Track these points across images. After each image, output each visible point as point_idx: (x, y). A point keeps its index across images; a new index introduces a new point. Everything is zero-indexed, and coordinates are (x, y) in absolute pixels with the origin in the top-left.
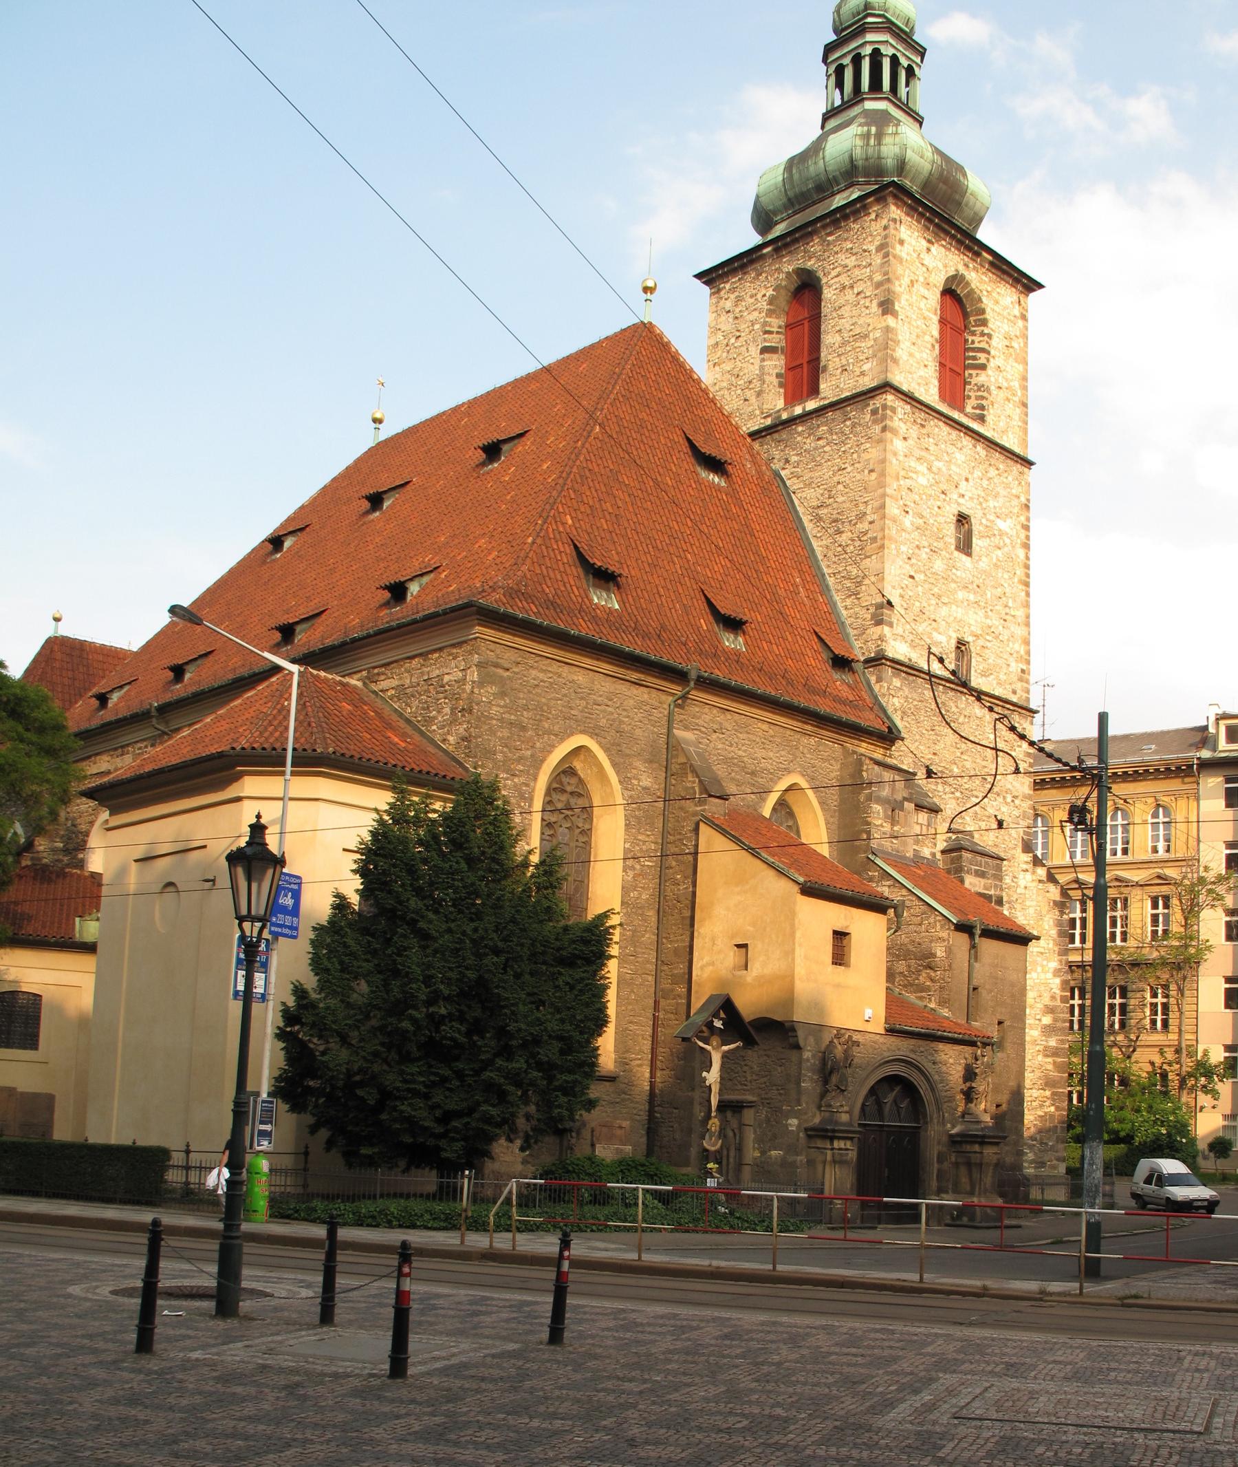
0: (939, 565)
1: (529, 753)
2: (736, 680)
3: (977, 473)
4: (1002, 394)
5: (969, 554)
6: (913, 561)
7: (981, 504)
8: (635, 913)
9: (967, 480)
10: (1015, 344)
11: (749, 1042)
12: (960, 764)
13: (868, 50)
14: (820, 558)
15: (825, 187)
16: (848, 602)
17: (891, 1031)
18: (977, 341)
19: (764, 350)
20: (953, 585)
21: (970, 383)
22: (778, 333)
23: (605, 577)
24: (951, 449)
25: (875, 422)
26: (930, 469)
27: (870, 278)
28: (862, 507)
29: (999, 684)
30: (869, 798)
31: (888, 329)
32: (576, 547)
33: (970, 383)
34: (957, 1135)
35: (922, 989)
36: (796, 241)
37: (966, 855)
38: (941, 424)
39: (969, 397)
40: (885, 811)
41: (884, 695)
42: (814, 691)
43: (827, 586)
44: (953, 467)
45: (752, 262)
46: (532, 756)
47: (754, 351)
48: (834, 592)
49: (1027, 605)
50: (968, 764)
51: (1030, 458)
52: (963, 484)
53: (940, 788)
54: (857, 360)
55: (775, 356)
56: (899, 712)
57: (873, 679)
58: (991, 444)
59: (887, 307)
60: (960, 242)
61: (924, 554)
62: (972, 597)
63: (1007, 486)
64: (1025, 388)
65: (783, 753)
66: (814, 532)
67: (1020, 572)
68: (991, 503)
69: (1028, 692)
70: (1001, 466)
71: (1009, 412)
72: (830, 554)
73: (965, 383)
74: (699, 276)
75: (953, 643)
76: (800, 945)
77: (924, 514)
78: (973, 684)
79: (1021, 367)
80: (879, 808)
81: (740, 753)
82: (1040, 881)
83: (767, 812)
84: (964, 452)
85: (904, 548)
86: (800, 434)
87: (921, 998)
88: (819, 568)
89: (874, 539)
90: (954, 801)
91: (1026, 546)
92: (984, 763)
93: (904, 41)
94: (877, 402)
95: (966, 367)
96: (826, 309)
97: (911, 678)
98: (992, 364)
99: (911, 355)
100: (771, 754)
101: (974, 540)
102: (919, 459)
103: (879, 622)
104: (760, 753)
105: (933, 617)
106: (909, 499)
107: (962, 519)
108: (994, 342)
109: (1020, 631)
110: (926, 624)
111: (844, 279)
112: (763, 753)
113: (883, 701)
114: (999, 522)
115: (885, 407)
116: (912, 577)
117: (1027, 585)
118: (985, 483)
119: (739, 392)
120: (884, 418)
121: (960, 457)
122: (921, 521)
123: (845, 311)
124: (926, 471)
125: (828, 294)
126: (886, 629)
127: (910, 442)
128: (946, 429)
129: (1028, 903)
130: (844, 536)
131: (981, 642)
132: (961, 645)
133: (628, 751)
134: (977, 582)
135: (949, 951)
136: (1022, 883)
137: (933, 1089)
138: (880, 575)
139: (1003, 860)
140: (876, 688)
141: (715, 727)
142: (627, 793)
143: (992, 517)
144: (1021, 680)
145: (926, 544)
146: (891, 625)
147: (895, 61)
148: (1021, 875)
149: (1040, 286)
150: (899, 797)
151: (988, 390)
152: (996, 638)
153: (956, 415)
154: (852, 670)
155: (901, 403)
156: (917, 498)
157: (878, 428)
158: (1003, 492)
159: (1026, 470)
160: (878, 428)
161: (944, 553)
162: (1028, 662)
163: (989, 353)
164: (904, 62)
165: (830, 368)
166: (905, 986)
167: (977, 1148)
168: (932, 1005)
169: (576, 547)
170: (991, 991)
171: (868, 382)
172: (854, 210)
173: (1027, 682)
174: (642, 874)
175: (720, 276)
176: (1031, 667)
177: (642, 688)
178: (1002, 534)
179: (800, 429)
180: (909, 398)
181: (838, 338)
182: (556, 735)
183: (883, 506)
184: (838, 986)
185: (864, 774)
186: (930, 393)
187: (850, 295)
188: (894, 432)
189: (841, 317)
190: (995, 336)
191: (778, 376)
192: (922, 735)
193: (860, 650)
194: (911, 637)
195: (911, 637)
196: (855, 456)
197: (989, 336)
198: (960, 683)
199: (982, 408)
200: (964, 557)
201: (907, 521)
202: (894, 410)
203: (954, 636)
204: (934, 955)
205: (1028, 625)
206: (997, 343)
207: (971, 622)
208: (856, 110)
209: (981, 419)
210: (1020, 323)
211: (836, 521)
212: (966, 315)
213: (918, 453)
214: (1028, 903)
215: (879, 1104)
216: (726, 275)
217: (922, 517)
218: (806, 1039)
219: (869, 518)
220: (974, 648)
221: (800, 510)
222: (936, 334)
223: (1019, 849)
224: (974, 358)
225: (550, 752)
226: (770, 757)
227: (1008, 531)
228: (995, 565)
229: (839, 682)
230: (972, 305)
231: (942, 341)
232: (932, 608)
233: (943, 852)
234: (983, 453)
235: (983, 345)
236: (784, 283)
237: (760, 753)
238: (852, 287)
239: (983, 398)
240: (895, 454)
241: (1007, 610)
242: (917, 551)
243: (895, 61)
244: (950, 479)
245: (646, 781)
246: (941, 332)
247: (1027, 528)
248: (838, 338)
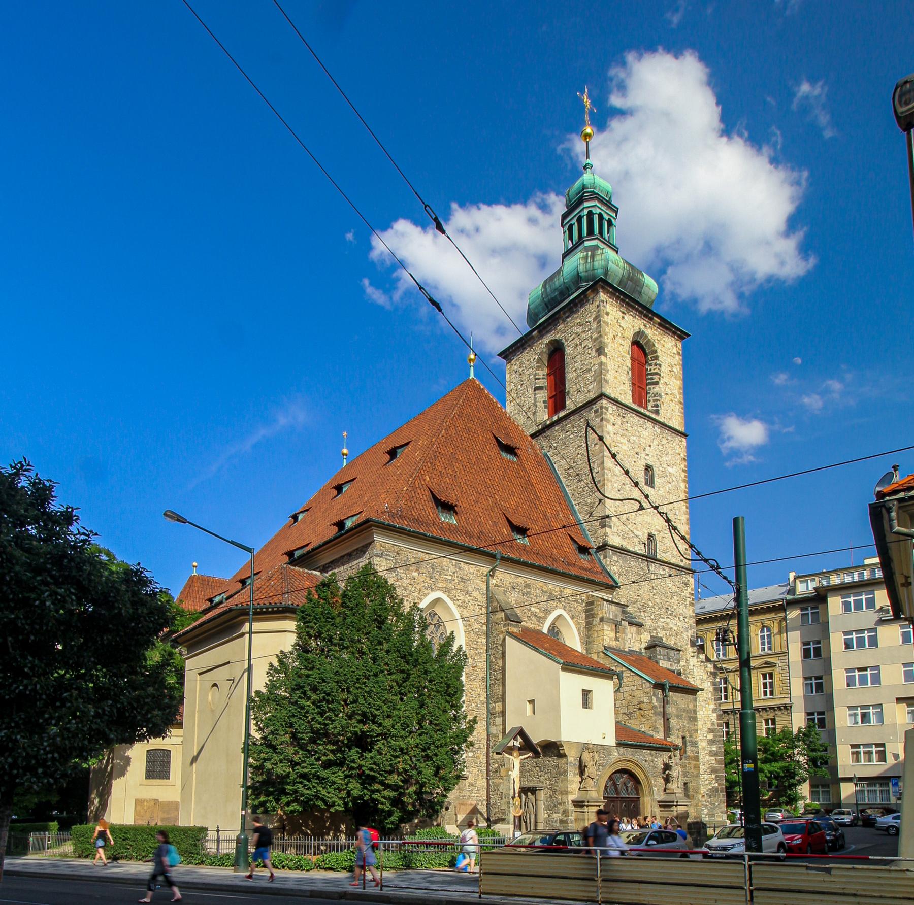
2: (523, 558)
3: (656, 442)
4: (668, 398)
11: (537, 754)
13: (586, 212)
15: (564, 292)
18: (652, 369)
23: (448, 507)
24: (640, 429)
25: (597, 417)
26: (629, 441)
27: (591, 337)
32: (431, 492)
42: (569, 564)
54: (586, 385)
57: (602, 557)
58: (664, 426)
60: (641, 313)
63: (673, 448)
73: (647, 393)
75: (646, 535)
78: (658, 557)
83: (545, 631)
84: (648, 431)
85: (615, 485)
93: (606, 205)
94: (597, 406)
96: (567, 359)
98: (662, 381)
99: (615, 378)
103: (603, 526)
107: (648, 468)
111: (577, 341)
113: (608, 568)
115: (601, 407)
118: (660, 447)
120: (602, 413)
121: (645, 434)
123: (578, 358)
125: (568, 351)
126: (608, 529)
131: (662, 534)
132: (650, 536)
140: (604, 562)
146: (611, 527)
147: (601, 217)
149: (688, 335)
151: (660, 395)
153: (642, 410)
157: (598, 420)
160: (598, 420)
164: (606, 217)
169: (431, 492)
171: (592, 396)
172: (581, 301)
180: (615, 401)
183: (603, 463)
186: (628, 400)
188: (608, 421)
189: (576, 362)
190: (663, 365)
193: (593, 543)
197: (660, 365)
199: (657, 406)
202: (607, 409)
206: (664, 369)
208: (581, 247)
209: (657, 412)
212: (646, 355)
213: (621, 432)
215: (615, 784)
222: (630, 366)
224: (652, 379)
229: (584, 560)
231: (632, 369)
233: (646, 649)
234: (659, 431)
238: (581, 344)
239: (657, 400)
240: (609, 433)
243: (601, 217)
246: (632, 365)
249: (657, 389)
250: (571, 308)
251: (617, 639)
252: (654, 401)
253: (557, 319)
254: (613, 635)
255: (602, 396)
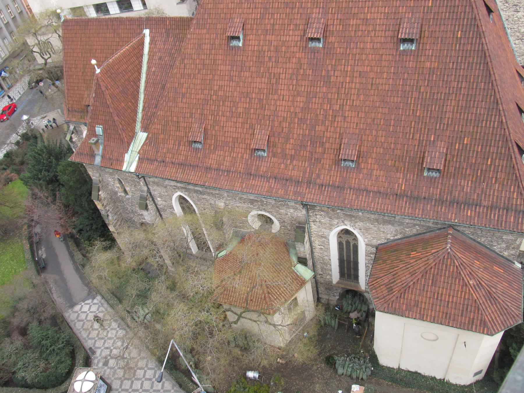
14: (504, 20)
16: (517, 42)
43: (506, 33)
48: (509, 36)
66: (502, 7)
72: (510, 19)
88: (503, 24)
130: (519, 14)
211: (516, 6)
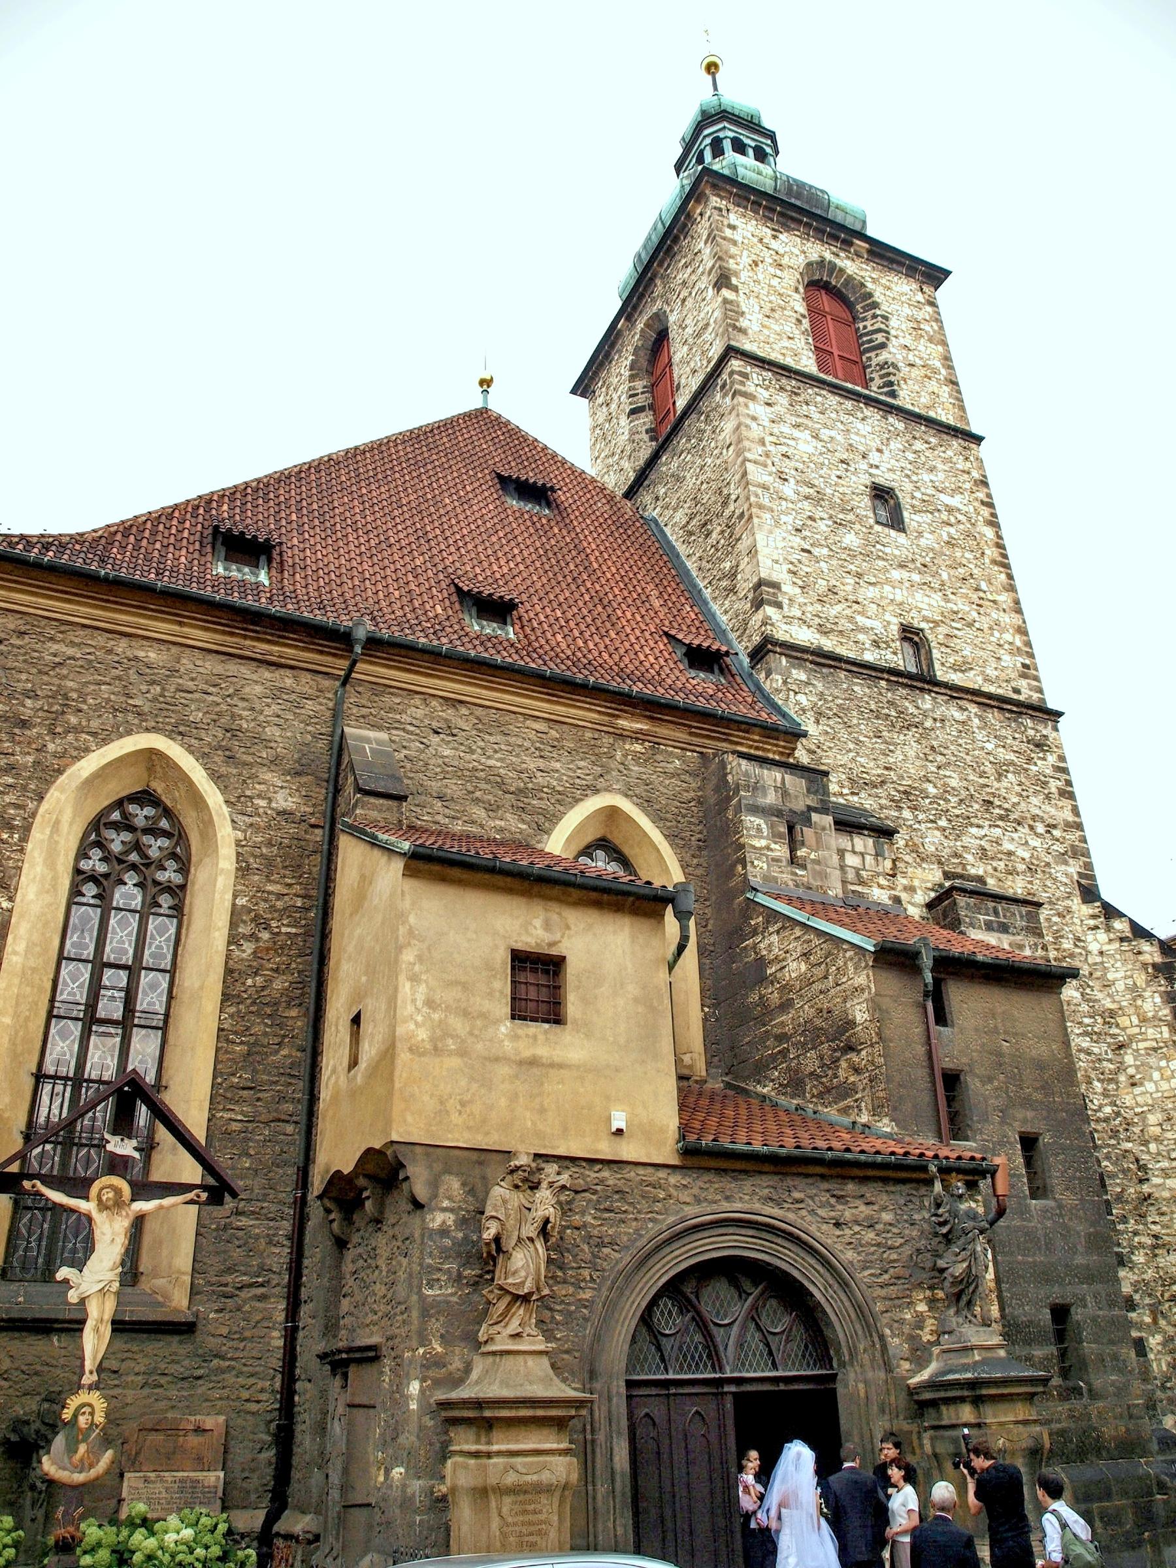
0: (850, 539)
1: (30, 759)
4: (915, 372)
5: (903, 530)
6: (806, 533)
7: (908, 476)
8: (257, 1014)
9: (879, 451)
10: (928, 328)
12: (939, 783)
17: (697, 1156)
19: (633, 412)
20: (881, 563)
21: (870, 366)
22: (643, 393)
24: (844, 417)
25: (724, 397)
26: (816, 437)
28: (725, 492)
29: (985, 680)
30: (738, 810)
31: (726, 301)
33: (870, 366)
34: (931, 1385)
35: (846, 1091)
36: (642, 296)
37: (962, 901)
38: (824, 392)
39: (872, 380)
40: (772, 827)
41: (778, 691)
44: (853, 436)
45: (612, 346)
46: (37, 763)
47: (624, 420)
49: (1012, 588)
50: (954, 783)
51: (975, 430)
52: (874, 457)
53: (906, 814)
55: (643, 415)
56: (810, 714)
59: (723, 280)
61: (822, 526)
62: (916, 577)
64: (951, 368)
65: (582, 764)
67: (991, 552)
68: (926, 477)
69: (1040, 691)
70: (932, 440)
71: (931, 390)
73: (865, 368)
74: (574, 391)
75: (894, 629)
76: (414, 979)
77: (816, 482)
79: (940, 348)
80: (758, 821)
81: (491, 762)
82: (1122, 940)
85: (789, 519)
86: (666, 464)
87: (845, 1111)
88: (695, 586)
89: (742, 515)
90: (937, 833)
91: (993, 523)
92: (981, 781)
95: (862, 353)
97: (825, 670)
100: (558, 765)
101: (906, 514)
102: (797, 426)
103: (758, 604)
104: (532, 764)
105: (854, 598)
106: (788, 466)
107: (881, 494)
108: (893, 323)
109: (1007, 619)
110: (839, 608)
111: (684, 293)
112: (541, 763)
114: (942, 496)
115: (732, 373)
116: (809, 552)
117: (1007, 566)
118: (911, 456)
119: (616, 467)
122: (811, 491)
124: (809, 438)
126: (770, 610)
127: (776, 408)
128: (833, 400)
129: (1110, 976)
130: (714, 535)
131: (943, 630)
133: (250, 759)
134: (920, 560)
135: (875, 1006)
136: (1094, 947)
137: (844, 1285)
138: (752, 552)
139: (1039, 905)
140: (766, 686)
141: (435, 725)
142: (240, 818)
143: (931, 491)
144: (1024, 676)
145: (826, 516)
146: (779, 605)
148: (1090, 937)
150: (799, 805)
151: (894, 366)
152: (970, 625)
154: (724, 670)
155: (757, 370)
156: (800, 466)
157: (728, 399)
158: (940, 466)
159: (973, 446)
160: (728, 399)
161: (857, 526)
162: (1031, 656)
163: (888, 333)
165: (683, 381)
166: (820, 1095)
167: (966, 1413)
168: (864, 1118)
170: (990, 1079)
173: (1036, 679)
174: (276, 947)
175: (592, 379)
176: (1038, 660)
177: (282, 671)
178: (950, 510)
179: (664, 459)
181: (686, 348)
182: (94, 734)
183: (745, 474)
184: (533, 1062)
185: (729, 778)
187: (689, 303)
191: (647, 432)
192: (858, 742)
194: (817, 621)
195: (817, 621)
196: (713, 445)
197: (887, 318)
198: (923, 681)
199: (891, 384)
200: (893, 533)
201: (788, 490)
203: (895, 620)
204: (852, 1023)
205: (1019, 611)
207: (925, 607)
209: (893, 394)
210: (929, 309)
212: (849, 305)
213: (794, 420)
214: (1110, 976)
216: (596, 373)
217: (813, 486)
218: (434, 1184)
219: (733, 497)
220: (934, 637)
221: (672, 538)
223: (1077, 900)
224: (871, 341)
225: (78, 758)
226: (562, 769)
227: (961, 507)
228: (948, 543)
230: (855, 293)
232: (849, 588)
234: (901, 426)
235: (876, 327)
236: (640, 344)
237: (532, 764)
238: (690, 293)
239: (889, 374)
240: (754, 419)
241: (982, 594)
242: (809, 522)
244: (851, 448)
245: (285, 800)
247: (990, 505)
248: (686, 348)
249: (884, 356)
250: (670, 248)
251: (793, 860)
252: (881, 377)
253: (652, 279)
254: (781, 850)
255: (731, 351)
